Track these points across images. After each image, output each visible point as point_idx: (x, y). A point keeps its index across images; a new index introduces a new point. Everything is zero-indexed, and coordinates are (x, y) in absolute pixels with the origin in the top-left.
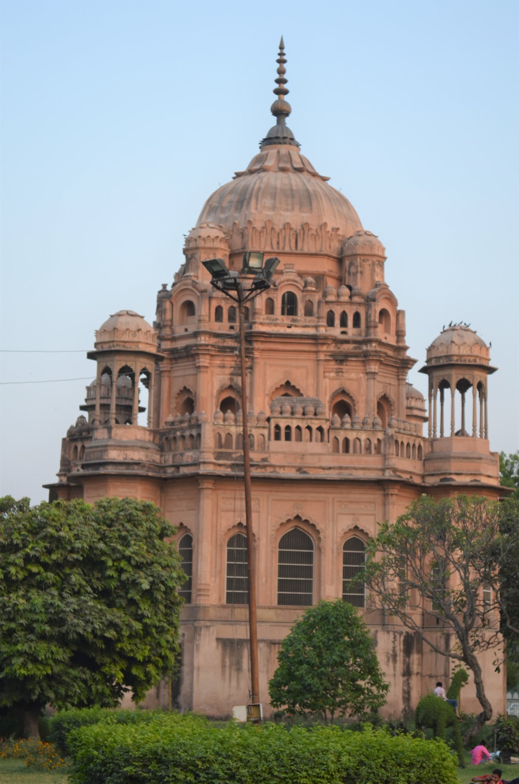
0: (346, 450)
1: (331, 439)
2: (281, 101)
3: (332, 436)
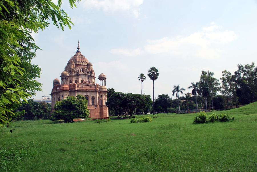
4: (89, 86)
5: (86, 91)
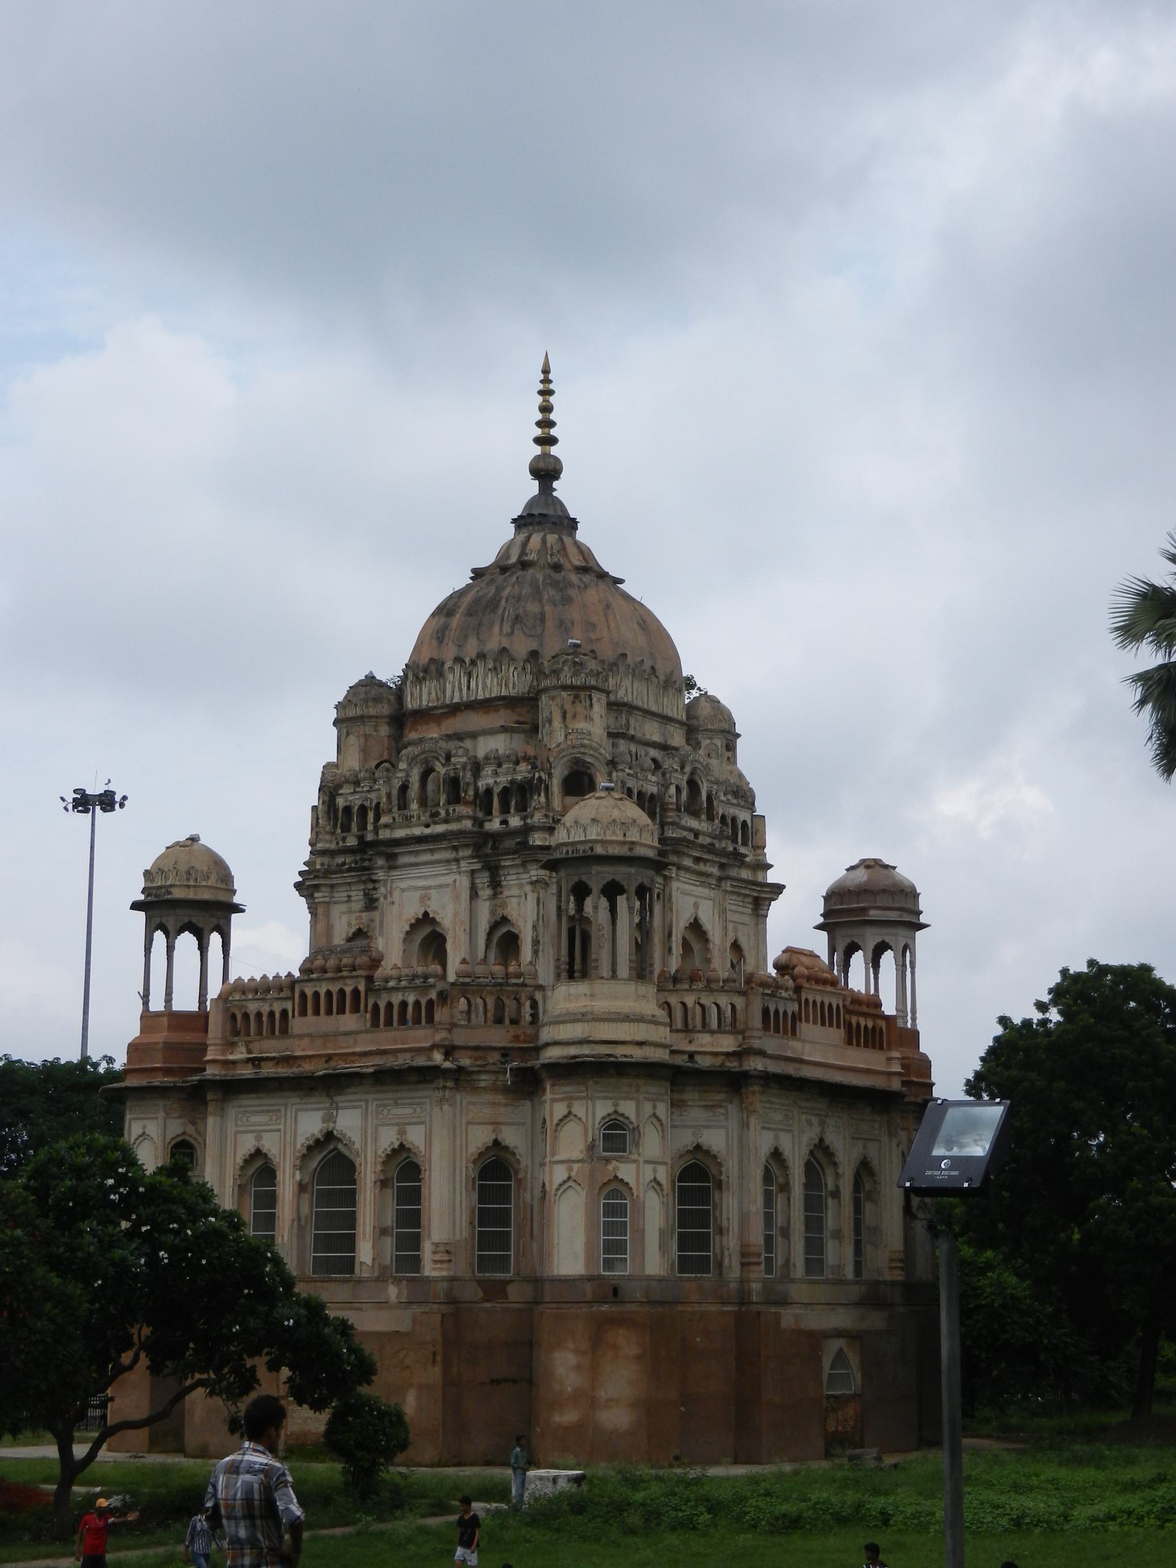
0: (403, 1021)
1: (370, 1008)
2: (546, 456)
3: (371, 1002)
4: (356, 1009)
5: (331, 1084)
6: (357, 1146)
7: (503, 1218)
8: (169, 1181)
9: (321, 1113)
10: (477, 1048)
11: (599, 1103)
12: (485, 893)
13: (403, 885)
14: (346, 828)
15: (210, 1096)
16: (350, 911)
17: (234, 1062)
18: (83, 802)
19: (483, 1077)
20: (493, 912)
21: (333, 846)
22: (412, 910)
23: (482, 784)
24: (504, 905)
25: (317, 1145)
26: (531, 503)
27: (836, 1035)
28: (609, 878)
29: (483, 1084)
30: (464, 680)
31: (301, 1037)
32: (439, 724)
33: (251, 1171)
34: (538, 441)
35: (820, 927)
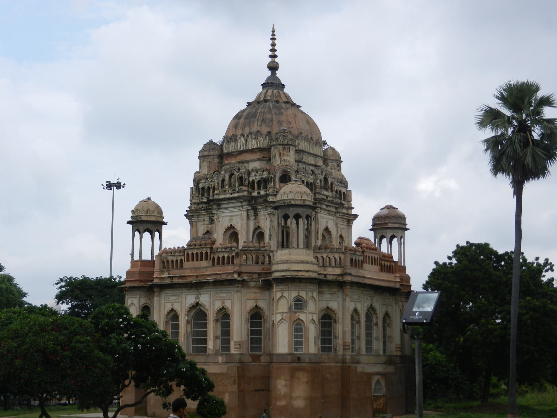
0: (223, 263)
2: (273, 62)
4: (207, 259)
5: (198, 285)
6: (208, 307)
7: (259, 333)
8: (141, 320)
9: (194, 296)
10: (249, 273)
11: (293, 292)
12: (252, 218)
13: (223, 215)
14: (203, 195)
15: (155, 290)
16: (204, 225)
17: (164, 278)
18: (110, 186)
19: (252, 283)
20: (255, 224)
21: (198, 201)
22: (227, 224)
23: (251, 179)
24: (259, 222)
25: (193, 307)
26: (268, 79)
27: (377, 268)
28: (296, 212)
29: (252, 286)
30: (244, 142)
31: (187, 269)
32: (236, 158)
33: (170, 316)
34: (271, 56)
35: (371, 230)
